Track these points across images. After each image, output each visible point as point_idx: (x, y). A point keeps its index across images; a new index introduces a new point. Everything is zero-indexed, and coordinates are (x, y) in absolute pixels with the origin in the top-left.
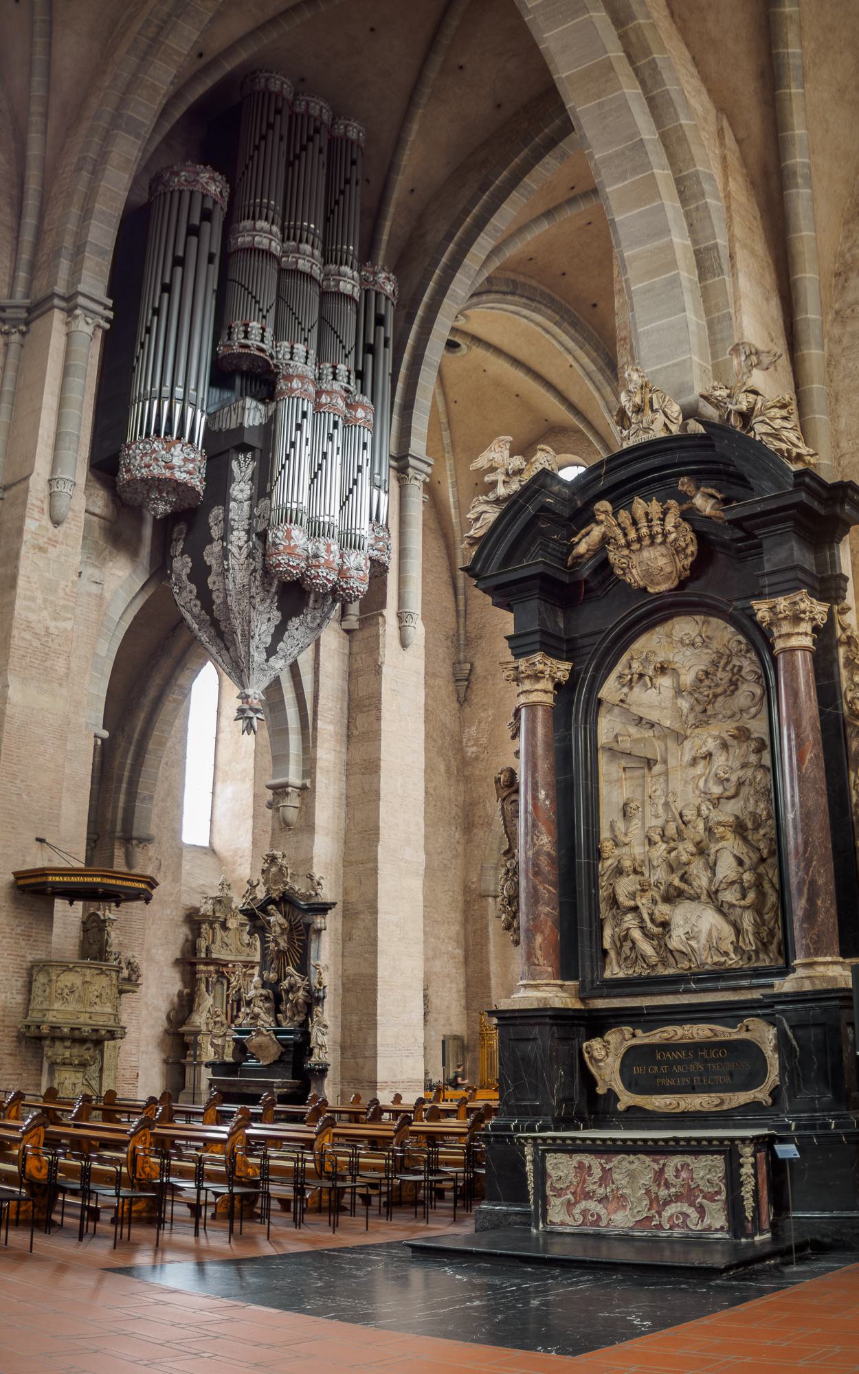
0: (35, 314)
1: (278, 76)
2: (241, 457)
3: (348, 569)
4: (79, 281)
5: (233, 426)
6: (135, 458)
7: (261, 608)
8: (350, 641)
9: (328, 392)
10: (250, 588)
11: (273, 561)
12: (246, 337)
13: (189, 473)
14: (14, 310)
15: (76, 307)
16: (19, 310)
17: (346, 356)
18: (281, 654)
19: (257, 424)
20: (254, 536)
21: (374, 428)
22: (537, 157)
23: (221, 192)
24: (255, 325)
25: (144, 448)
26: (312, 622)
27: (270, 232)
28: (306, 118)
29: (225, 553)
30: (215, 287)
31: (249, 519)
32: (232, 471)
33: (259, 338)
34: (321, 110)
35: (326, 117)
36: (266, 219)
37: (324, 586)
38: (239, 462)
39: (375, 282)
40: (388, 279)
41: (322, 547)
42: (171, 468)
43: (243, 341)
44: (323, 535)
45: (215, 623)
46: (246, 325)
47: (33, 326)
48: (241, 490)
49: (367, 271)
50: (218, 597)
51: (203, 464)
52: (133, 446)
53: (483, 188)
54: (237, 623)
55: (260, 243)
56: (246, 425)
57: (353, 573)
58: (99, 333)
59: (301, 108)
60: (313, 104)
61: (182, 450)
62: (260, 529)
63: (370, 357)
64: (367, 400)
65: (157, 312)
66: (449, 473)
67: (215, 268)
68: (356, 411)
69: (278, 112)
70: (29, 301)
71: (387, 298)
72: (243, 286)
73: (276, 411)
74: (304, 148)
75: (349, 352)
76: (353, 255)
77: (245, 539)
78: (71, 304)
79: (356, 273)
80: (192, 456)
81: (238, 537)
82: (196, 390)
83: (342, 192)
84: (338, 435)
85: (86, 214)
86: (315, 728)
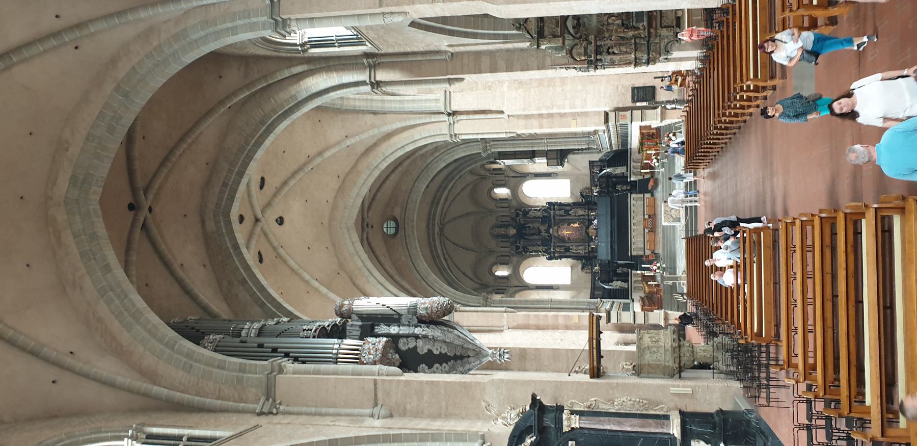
2: (376, 331)
5: (359, 333)
6: (369, 358)
10: (444, 330)
15: (280, 365)
16: (265, 405)
20: (419, 324)
22: (240, 254)
24: (304, 328)
29: (425, 337)
31: (409, 326)
42: (380, 342)
45: (456, 358)
46: (304, 330)
48: (394, 330)
50: (444, 349)
52: (362, 360)
53: (244, 282)
54: (457, 342)
62: (415, 321)
70: (263, 397)
73: (357, 314)
77: (419, 328)
78: (277, 368)
81: (418, 331)
85: (221, 366)
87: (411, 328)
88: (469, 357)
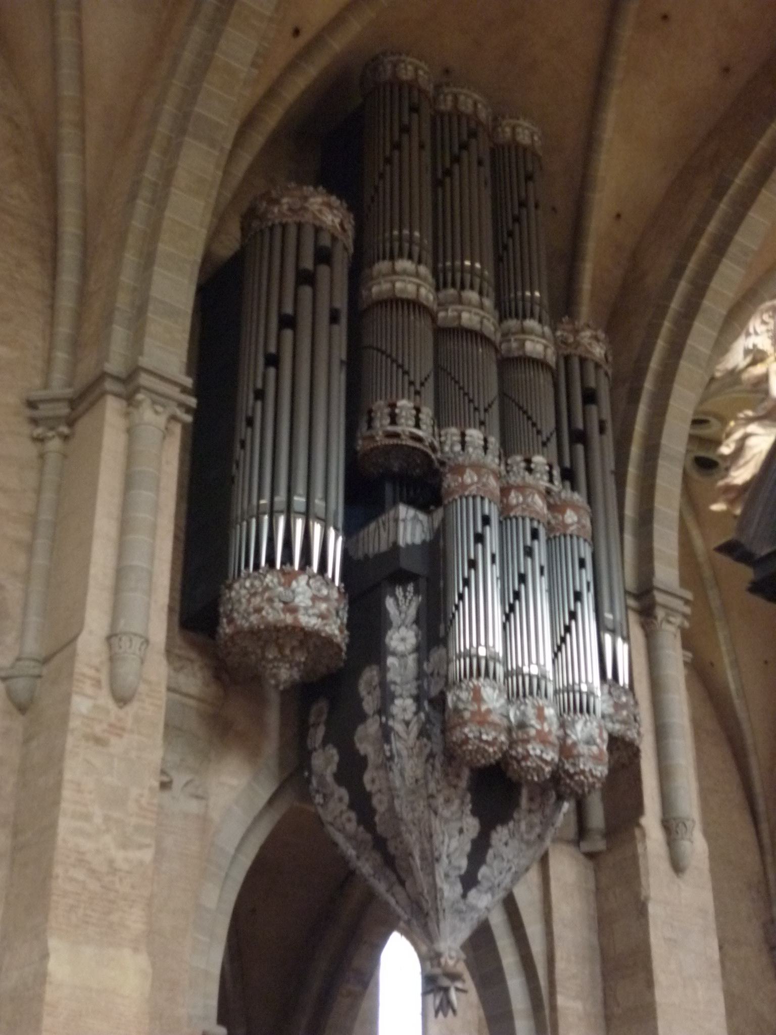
0: (81, 408)
1: (409, 59)
2: (399, 591)
3: (575, 744)
4: (141, 353)
5: (384, 547)
6: (239, 601)
7: (446, 813)
8: (596, 871)
9: (521, 489)
10: (427, 784)
11: (456, 736)
12: (394, 422)
13: (322, 616)
14: (50, 406)
15: (138, 389)
17: (544, 444)
18: (485, 884)
19: (418, 540)
20: (426, 704)
21: (594, 538)
23: (341, 225)
24: (405, 404)
25: (252, 585)
26: (529, 832)
27: (417, 275)
28: (455, 119)
29: (386, 733)
30: (344, 357)
32: (386, 612)
33: (412, 422)
34: (475, 104)
35: (483, 115)
36: (410, 257)
37: (539, 770)
38: (396, 599)
39: (577, 344)
40: (596, 338)
41: (531, 712)
42: (294, 610)
43: (391, 428)
44: (531, 693)
45: (380, 844)
46: (393, 406)
47: (80, 426)
49: (564, 330)
50: (380, 802)
51: (344, 606)
53: (719, 193)
54: (412, 839)
55: (403, 290)
56: (401, 543)
57: (583, 749)
58: (177, 429)
59: (446, 105)
60: (462, 98)
61: (308, 584)
62: (434, 692)
63: (580, 448)
64: (579, 498)
65: (260, 395)
66: (724, 648)
67: (341, 331)
68: (563, 513)
69: (414, 109)
71: (597, 366)
72: (383, 353)
73: (444, 521)
74: (456, 159)
75: (548, 439)
76: (540, 305)
79: (547, 330)
80: (325, 592)
82: (326, 498)
83: (517, 219)
84: (540, 549)
86: (554, 1008)
87: (415, 684)
88: (402, 883)
